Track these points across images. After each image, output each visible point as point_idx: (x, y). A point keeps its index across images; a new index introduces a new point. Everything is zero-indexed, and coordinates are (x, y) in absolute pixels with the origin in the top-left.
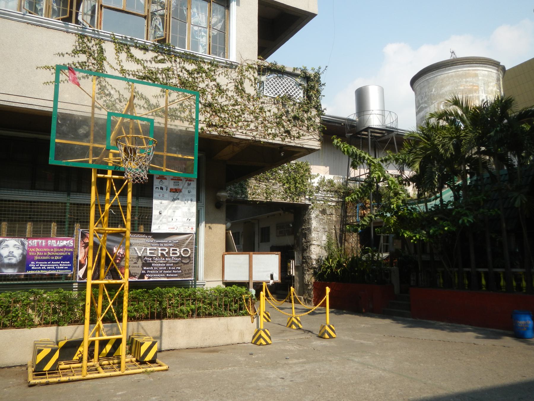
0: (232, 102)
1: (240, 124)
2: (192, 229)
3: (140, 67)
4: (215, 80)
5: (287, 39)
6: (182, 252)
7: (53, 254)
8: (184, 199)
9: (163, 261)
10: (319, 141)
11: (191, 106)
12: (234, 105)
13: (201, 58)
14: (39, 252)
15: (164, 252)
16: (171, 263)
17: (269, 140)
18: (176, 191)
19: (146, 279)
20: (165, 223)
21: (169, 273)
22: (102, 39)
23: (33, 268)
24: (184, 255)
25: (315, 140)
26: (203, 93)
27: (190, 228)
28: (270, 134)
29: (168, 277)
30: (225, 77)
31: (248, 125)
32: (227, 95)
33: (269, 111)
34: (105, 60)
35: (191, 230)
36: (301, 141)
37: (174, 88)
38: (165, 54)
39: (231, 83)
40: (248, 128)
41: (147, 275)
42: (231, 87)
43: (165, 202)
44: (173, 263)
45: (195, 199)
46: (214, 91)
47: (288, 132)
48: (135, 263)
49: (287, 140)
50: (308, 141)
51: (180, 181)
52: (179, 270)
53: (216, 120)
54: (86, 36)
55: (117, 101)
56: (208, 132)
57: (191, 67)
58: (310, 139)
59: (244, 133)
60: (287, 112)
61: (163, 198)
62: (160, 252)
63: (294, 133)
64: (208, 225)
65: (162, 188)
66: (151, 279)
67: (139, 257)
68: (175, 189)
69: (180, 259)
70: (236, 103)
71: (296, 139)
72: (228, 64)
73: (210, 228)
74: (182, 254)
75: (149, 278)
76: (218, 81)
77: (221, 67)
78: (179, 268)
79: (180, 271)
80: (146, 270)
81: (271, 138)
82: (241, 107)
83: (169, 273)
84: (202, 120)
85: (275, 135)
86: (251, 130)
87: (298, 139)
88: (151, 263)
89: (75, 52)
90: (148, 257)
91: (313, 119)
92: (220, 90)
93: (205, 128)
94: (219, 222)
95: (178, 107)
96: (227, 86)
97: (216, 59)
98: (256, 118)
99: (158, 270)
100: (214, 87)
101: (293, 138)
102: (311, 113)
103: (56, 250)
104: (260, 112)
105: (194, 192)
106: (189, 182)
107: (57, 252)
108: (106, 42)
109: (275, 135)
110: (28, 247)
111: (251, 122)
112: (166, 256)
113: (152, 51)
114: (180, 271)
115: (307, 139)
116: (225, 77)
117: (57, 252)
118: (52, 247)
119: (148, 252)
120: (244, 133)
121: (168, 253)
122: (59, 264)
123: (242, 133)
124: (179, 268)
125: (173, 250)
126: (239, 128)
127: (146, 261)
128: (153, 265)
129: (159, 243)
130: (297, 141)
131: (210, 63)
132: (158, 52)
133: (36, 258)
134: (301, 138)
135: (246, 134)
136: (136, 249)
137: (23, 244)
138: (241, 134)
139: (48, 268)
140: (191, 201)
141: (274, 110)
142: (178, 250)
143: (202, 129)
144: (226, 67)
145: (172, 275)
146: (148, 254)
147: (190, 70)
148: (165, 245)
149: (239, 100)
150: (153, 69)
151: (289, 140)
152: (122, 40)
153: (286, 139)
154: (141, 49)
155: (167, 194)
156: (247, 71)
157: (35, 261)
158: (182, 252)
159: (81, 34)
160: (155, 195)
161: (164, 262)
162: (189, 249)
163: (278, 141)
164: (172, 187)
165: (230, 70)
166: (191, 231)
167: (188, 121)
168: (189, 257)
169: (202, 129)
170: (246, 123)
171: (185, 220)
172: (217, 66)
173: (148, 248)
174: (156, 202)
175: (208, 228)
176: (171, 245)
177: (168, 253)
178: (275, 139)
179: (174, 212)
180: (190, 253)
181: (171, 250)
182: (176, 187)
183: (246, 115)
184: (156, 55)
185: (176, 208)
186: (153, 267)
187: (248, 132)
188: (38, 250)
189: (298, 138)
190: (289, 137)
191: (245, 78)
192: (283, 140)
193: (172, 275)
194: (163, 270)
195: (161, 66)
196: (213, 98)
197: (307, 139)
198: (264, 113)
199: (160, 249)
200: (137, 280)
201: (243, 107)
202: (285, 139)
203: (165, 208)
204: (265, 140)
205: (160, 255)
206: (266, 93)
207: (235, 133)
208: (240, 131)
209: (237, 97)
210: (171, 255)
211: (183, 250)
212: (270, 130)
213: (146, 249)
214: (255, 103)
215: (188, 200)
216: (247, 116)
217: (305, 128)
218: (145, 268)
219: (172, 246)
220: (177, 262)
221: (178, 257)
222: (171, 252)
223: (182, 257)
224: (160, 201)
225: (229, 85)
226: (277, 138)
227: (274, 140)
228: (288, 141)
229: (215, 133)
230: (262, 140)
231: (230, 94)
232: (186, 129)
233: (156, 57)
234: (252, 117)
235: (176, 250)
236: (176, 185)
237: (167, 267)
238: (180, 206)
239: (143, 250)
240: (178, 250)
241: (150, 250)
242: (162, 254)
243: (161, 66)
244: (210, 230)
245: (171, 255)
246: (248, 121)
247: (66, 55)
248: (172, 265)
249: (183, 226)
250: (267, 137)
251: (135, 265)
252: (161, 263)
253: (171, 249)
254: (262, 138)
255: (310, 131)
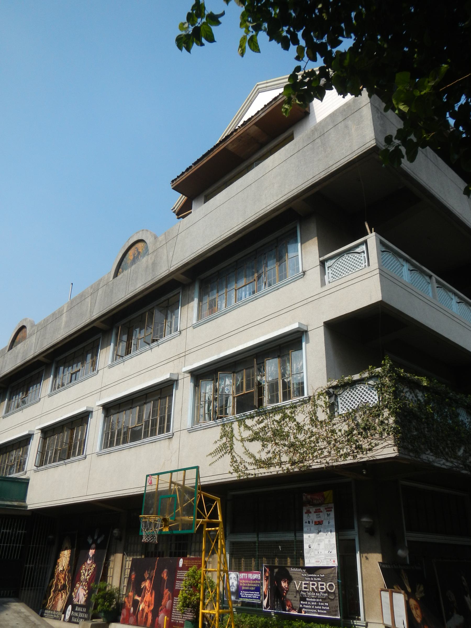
0: (309, 434)
1: (315, 454)
2: (334, 561)
3: (251, 432)
4: (295, 420)
5: (413, 319)
6: (327, 587)
7: (251, 585)
8: (325, 530)
9: (314, 596)
10: (395, 446)
11: (280, 452)
12: (310, 437)
13: (284, 406)
14: (245, 583)
15: (314, 587)
16: (319, 599)
17: (341, 462)
18: (319, 523)
19: (303, 614)
20: (313, 557)
21: (320, 609)
22: (232, 422)
23: (242, 596)
24: (330, 591)
25: (390, 446)
26: (287, 436)
27: (332, 560)
28: (342, 455)
29: (319, 613)
30: (302, 413)
31: (322, 453)
32: (305, 430)
33: (340, 431)
34: (233, 436)
35: (333, 563)
36: (374, 453)
37: (269, 440)
38: (263, 414)
39: (307, 417)
40: (323, 456)
41: (304, 609)
42: (308, 421)
43: (312, 535)
44: (322, 599)
45: (334, 529)
46: (295, 431)
47: (359, 447)
48: (295, 597)
49: (359, 456)
50: (382, 449)
51: (321, 514)
52: (327, 606)
53: (296, 458)
54: (225, 424)
55: (240, 464)
56: (291, 471)
57: (278, 417)
58: (384, 447)
59: (319, 462)
60: (357, 425)
61: (310, 532)
62: (311, 586)
63: (366, 446)
64: (364, 555)
65: (309, 522)
66: (306, 614)
67: (297, 592)
68: (318, 521)
69: (326, 594)
70: (312, 434)
71: (368, 452)
72: (302, 401)
73: (367, 558)
74: (328, 589)
75: (305, 612)
76: (297, 420)
77: (299, 406)
78: (327, 604)
79: (328, 608)
80: (303, 604)
81: (343, 459)
82: (316, 437)
83: (320, 609)
84: (288, 460)
85: (346, 455)
86: (325, 457)
87: (370, 452)
88: (306, 598)
89: (221, 438)
90: (303, 591)
91: (386, 422)
92: (300, 428)
93: (290, 468)
94: (375, 552)
95: (271, 456)
96: (304, 421)
97: (293, 402)
98: (329, 443)
99: (311, 605)
100: (294, 427)
101: (365, 453)
102: (383, 415)
103: (252, 582)
104: (332, 435)
105: (333, 522)
106: (328, 513)
107: (252, 583)
108: (234, 423)
109: (346, 455)
110: (240, 579)
111: (325, 448)
112: (316, 590)
113: (256, 416)
114: (328, 608)
115: (381, 448)
116: (302, 413)
117: (252, 583)
118: (249, 580)
119: (303, 586)
120: (319, 462)
121: (317, 588)
122: (253, 594)
123: (317, 462)
124: (327, 604)
125: (321, 585)
126: (315, 458)
127: (302, 595)
128: (307, 599)
129: (310, 577)
130: (370, 454)
131: (290, 407)
132: (259, 416)
133: (243, 588)
134: (373, 449)
135: (320, 462)
136: (296, 583)
137: (237, 577)
138: (317, 464)
139: (253, 597)
140: (331, 532)
141: (346, 428)
142: (325, 585)
143: (288, 469)
144: (302, 404)
145: (322, 611)
146: (304, 589)
147: (278, 419)
148: (315, 579)
149: (314, 430)
150: (257, 430)
151: (361, 455)
152: (240, 417)
153: (358, 455)
154: (250, 418)
155: (313, 527)
156: (319, 399)
157: (243, 590)
158: (327, 587)
159: (223, 424)
160: (305, 529)
161: (315, 597)
162: (333, 584)
163: (350, 460)
164: (316, 519)
165: (305, 405)
166: (333, 564)
167: (278, 465)
168: (334, 593)
169: (288, 469)
170: (320, 452)
171: (326, 552)
172: (295, 407)
173: (303, 582)
174: (306, 536)
175: (365, 558)
176: (319, 579)
177: (317, 588)
178: (347, 459)
179: (319, 544)
180: (334, 588)
181: (319, 585)
182: (319, 520)
183: (320, 444)
184: (259, 418)
185: (320, 541)
186: (308, 601)
187: (322, 460)
188: (244, 581)
189: (370, 450)
190: (361, 453)
191: (317, 407)
192: (355, 457)
193: (322, 611)
194: (315, 605)
195: (262, 425)
196: (295, 438)
197: (381, 448)
198: (335, 435)
199: (311, 583)
200: (297, 613)
201: (317, 436)
202: (356, 456)
203: (313, 542)
204: (338, 463)
205: (311, 590)
206: (342, 412)
207: (311, 464)
208: (315, 461)
209: (312, 428)
210: (320, 590)
211: (328, 584)
212: (341, 451)
213: (302, 583)
214: (327, 428)
215: (327, 531)
216: (322, 444)
217: (377, 436)
218: (302, 602)
219: (319, 581)
220: (324, 597)
221: (325, 592)
222: (320, 587)
223: (329, 593)
224: (309, 535)
225: (306, 420)
226: (350, 458)
227: (346, 460)
228: (363, 457)
229: (296, 470)
230: (335, 464)
231: (306, 428)
232: (277, 473)
233: (259, 420)
234: (325, 443)
235: (323, 585)
236: (318, 518)
237: (317, 602)
238: (323, 538)
239: (300, 584)
240: (325, 585)
241: (305, 584)
242: (312, 588)
243: (262, 425)
244: (367, 561)
245: (320, 590)
246: (322, 449)
247: (218, 442)
248: (321, 600)
249: (325, 559)
250: (340, 460)
251: (295, 599)
252: (313, 598)
253: (319, 583)
254: (334, 462)
255: (384, 437)
